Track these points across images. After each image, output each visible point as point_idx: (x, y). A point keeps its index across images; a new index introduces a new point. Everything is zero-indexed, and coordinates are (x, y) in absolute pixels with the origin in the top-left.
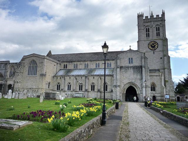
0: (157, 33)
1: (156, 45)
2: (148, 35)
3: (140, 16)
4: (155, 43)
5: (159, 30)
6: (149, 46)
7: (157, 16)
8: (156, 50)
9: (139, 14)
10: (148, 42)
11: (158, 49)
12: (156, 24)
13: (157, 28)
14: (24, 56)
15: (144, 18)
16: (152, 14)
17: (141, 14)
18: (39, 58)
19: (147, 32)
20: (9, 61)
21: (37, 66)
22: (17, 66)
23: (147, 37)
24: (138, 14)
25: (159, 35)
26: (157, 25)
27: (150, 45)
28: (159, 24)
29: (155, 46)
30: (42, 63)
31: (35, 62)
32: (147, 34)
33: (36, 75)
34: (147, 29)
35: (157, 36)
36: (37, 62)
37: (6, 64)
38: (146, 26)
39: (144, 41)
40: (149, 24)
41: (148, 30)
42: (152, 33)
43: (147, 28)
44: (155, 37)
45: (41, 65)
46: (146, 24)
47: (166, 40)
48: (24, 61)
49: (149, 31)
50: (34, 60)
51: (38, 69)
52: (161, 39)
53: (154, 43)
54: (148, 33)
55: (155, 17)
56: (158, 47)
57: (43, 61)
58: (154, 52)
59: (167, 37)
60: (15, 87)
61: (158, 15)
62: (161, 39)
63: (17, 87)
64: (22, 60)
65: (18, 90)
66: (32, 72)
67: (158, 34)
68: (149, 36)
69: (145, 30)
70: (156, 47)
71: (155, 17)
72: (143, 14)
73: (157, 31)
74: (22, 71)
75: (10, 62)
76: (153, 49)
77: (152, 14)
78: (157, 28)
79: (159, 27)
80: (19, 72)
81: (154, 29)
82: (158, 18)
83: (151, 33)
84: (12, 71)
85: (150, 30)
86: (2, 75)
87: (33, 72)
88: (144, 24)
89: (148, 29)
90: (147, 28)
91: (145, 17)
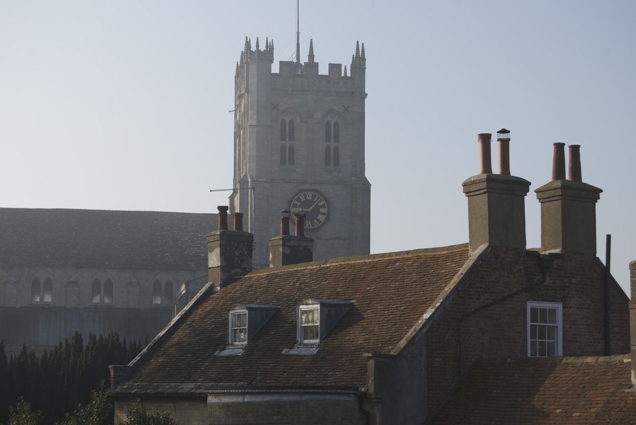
0: (328, 149)
1: (323, 206)
3: (255, 59)
5: (337, 139)
9: (254, 48)
13: (328, 124)
15: (275, 69)
16: (311, 56)
19: (283, 138)
23: (283, 161)
24: (248, 44)
25: (337, 164)
32: (283, 148)
34: (283, 123)
35: (328, 163)
43: (287, 120)
47: (366, 187)
49: (292, 138)
53: (314, 196)
54: (287, 144)
55: (323, 70)
56: (328, 219)
59: (369, 174)
68: (292, 162)
70: (321, 217)
71: (323, 70)
73: (328, 139)
77: (311, 56)
78: (328, 124)
79: (336, 124)
89: (292, 123)
90: (287, 120)
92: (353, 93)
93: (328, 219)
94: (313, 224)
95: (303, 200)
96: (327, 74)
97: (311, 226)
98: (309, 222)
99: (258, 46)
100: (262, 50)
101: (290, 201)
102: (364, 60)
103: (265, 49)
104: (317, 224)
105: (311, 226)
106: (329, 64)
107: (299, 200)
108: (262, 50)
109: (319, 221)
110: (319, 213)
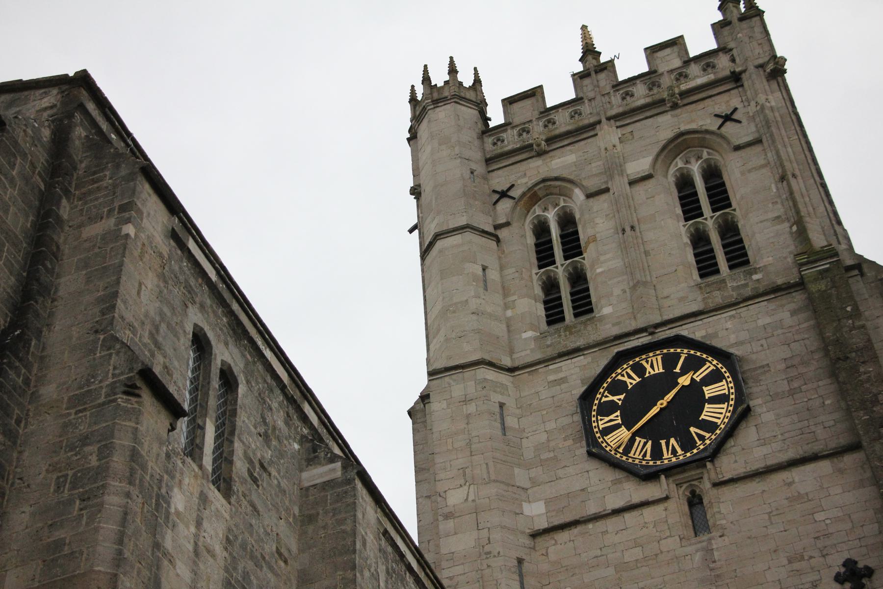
1: (715, 377)
2: (567, 300)
4: (693, 364)
6: (603, 422)
7: (652, 51)
8: (729, 464)
10: (577, 372)
11: (748, 434)
12: (667, 134)
17: (439, 78)
23: (554, 315)
26: (680, 144)
27: (607, 409)
28: (713, 124)
29: (693, 398)
34: (541, 230)
38: (532, 197)
39: (504, 378)
40: (562, 162)
41: (559, 244)
42: (624, 248)
43: (551, 217)
44: (677, 288)
46: (526, 174)
52: (776, 290)
53: (669, 362)
56: (742, 414)
58: (695, 501)
61: (677, 43)
62: (776, 290)
67: (719, 250)
69: (521, 241)
72: (477, 81)
76: (672, 451)
78: (684, 183)
81: (640, 190)
82: (681, 75)
83: (602, 262)
85: (597, 224)
88: (500, 180)
91: (509, 102)
92: (736, 78)
93: (742, 414)
94: (687, 443)
95: (632, 381)
96: (645, 69)
97: (680, 452)
98: (673, 441)
99: (426, 79)
100: (440, 84)
101: (587, 397)
102: (760, 13)
103: (447, 78)
104: (702, 438)
105: (680, 452)
106: (646, 49)
107: (617, 387)
108: (440, 84)
109: (710, 427)
110: (701, 401)
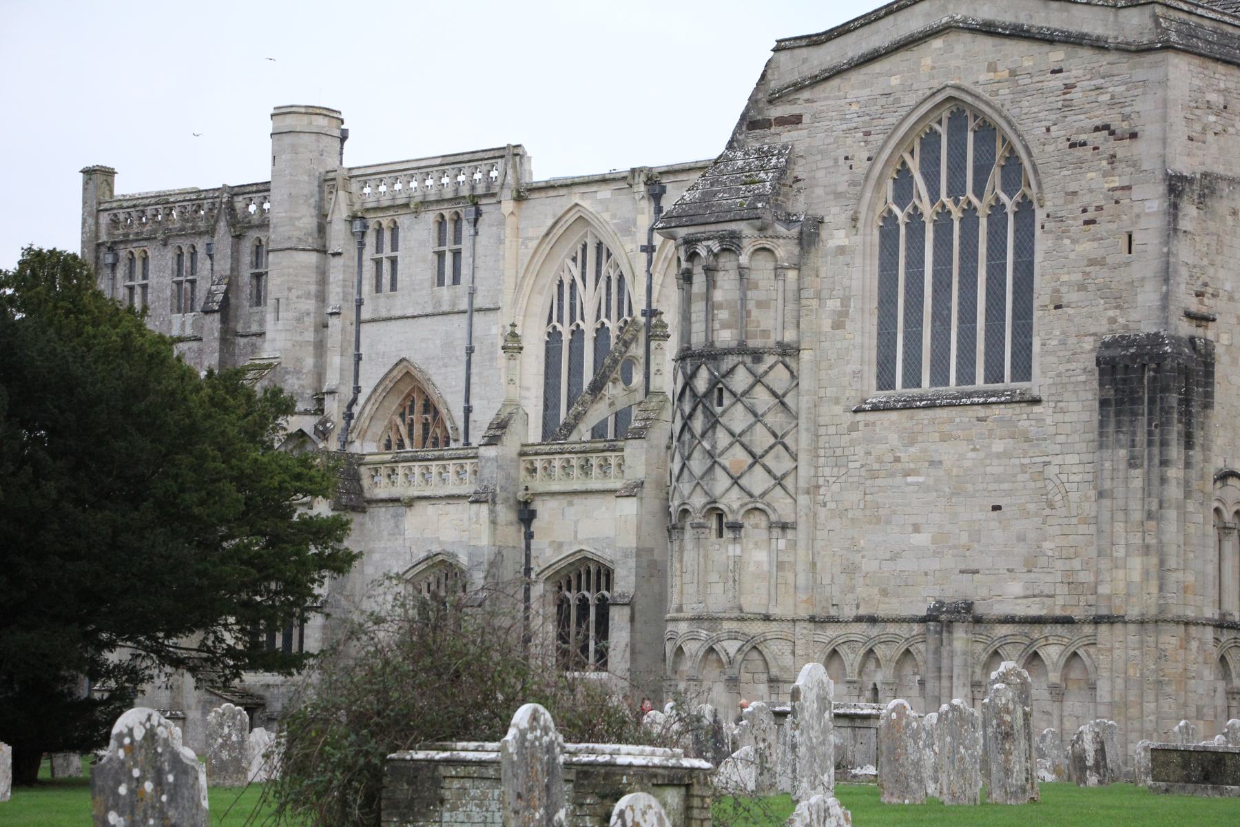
14: (781, 47)
18: (1057, 55)
20: (513, 155)
21: (1025, 210)
22: (690, 242)
30: (1122, 149)
31: (987, 132)
33: (1023, 370)
36: (1035, 123)
37: (474, 204)
45: (1095, 181)
48: (787, 136)
50: (958, 110)
51: (1057, 260)
57: (1145, 106)
60: (685, 594)
63: (718, 600)
64: (751, 122)
65: (732, 647)
66: (941, 318)
74: (770, 325)
75: (540, 173)
80: (725, 337)
84: (578, 334)
86: (429, 406)
87: (968, 316)
